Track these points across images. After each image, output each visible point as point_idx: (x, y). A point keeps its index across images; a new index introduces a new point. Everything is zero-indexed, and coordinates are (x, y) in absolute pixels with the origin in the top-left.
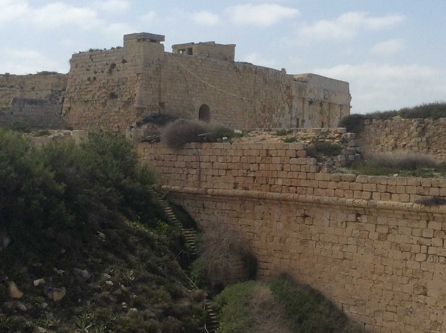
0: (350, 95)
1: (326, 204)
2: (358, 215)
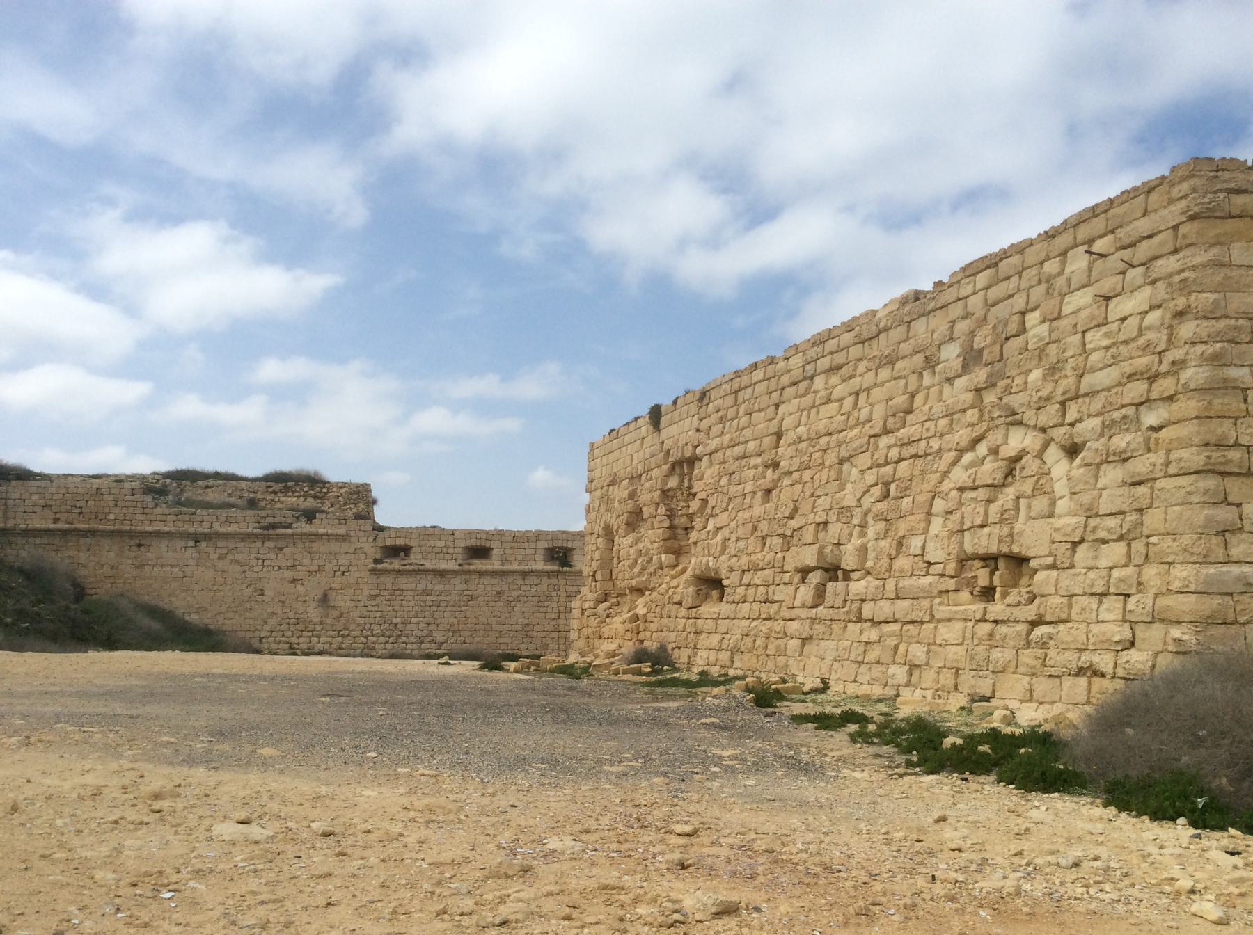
2: (197, 542)
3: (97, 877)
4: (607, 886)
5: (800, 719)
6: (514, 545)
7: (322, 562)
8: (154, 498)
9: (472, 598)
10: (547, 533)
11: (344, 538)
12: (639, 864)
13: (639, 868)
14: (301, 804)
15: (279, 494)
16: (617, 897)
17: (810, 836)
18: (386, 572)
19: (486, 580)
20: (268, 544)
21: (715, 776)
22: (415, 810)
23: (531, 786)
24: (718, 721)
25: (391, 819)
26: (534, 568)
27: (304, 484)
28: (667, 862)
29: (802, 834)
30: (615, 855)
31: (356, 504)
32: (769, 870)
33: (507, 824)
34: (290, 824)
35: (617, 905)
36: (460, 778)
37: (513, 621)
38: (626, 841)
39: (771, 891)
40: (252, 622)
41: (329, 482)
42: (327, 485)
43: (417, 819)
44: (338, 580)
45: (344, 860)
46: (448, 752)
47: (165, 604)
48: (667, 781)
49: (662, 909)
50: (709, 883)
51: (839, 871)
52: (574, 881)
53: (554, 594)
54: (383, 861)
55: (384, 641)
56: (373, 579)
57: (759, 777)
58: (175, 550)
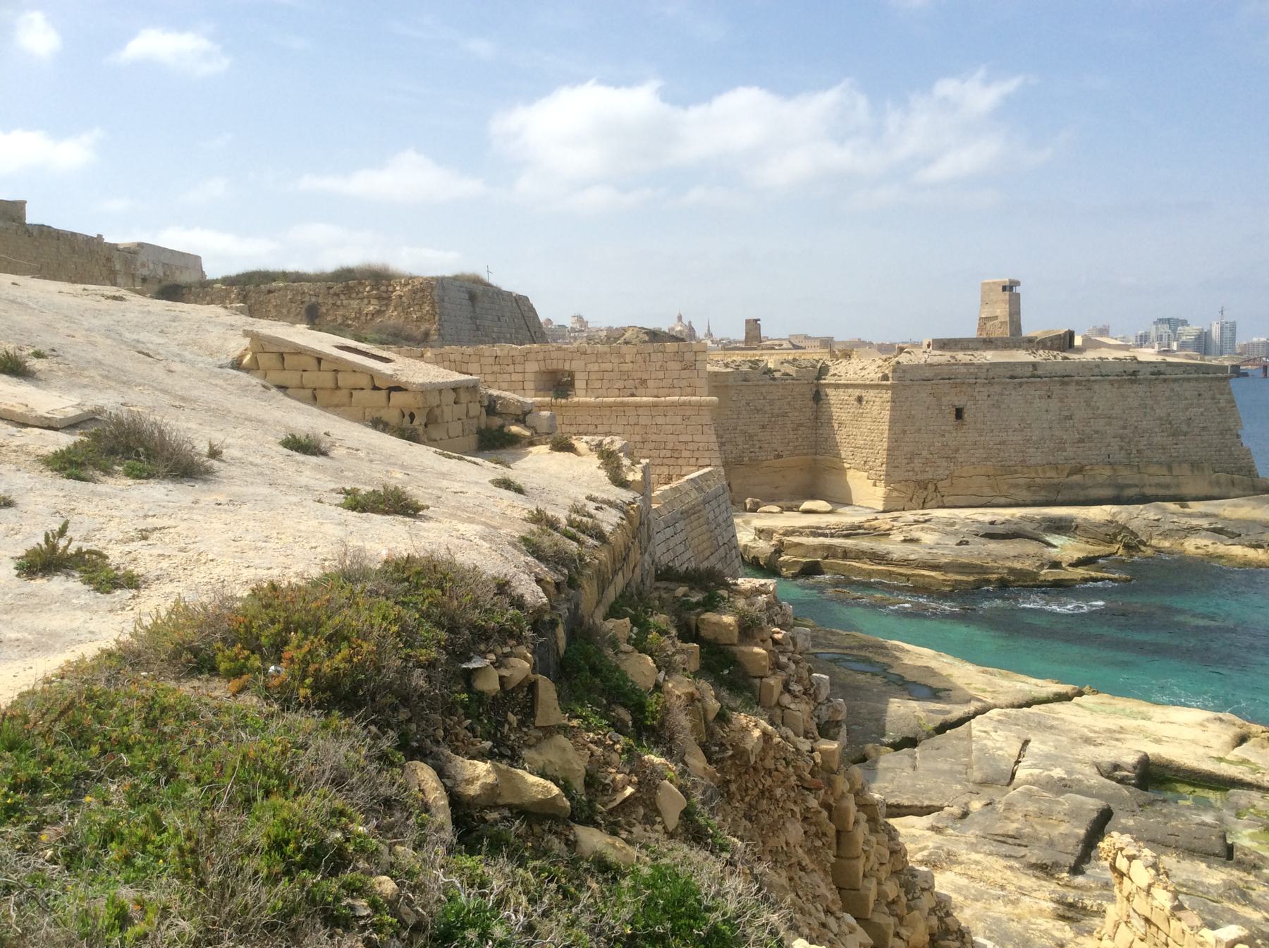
0: (203, 272)
6: (496, 368)
15: (342, 297)
31: (421, 305)
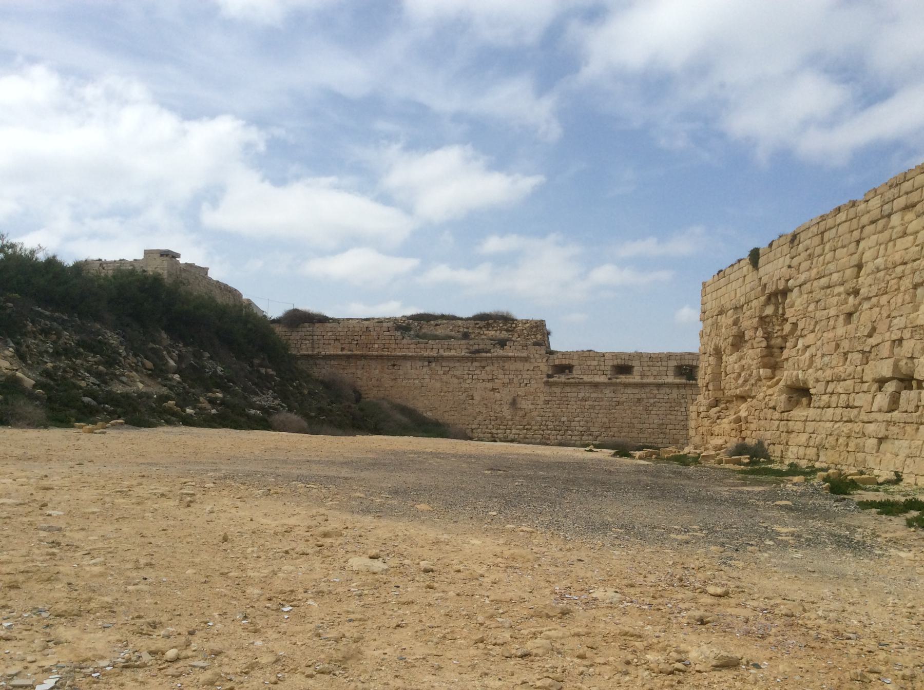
1: (410, 357)
2: (429, 362)
3: (248, 591)
4: (627, 633)
5: (865, 505)
7: (511, 377)
8: (402, 333)
9: (618, 403)
10: (676, 355)
11: (526, 359)
12: (663, 617)
13: (664, 620)
14: (422, 547)
15: (484, 329)
16: (633, 643)
17: (836, 605)
18: (556, 384)
19: (629, 390)
20: (475, 364)
21: (769, 548)
22: (502, 558)
23: (604, 545)
24: (791, 504)
25: (481, 563)
26: (666, 381)
27: (500, 322)
28: (690, 617)
29: (828, 602)
30: (646, 607)
31: (535, 335)
32: (781, 632)
33: (567, 575)
34: (406, 562)
35: (631, 650)
36: (549, 535)
37: (651, 421)
38: (662, 596)
39: (776, 650)
40: (466, 418)
41: (516, 320)
42: (515, 322)
43: (500, 565)
44: (523, 389)
45: (429, 592)
46: (551, 515)
47: (410, 405)
48: (722, 550)
49: (668, 657)
50: (721, 638)
51: (849, 638)
52: (602, 625)
53: (683, 401)
54: (458, 595)
55: (556, 433)
56: (547, 389)
57: (808, 551)
58: (416, 368)
